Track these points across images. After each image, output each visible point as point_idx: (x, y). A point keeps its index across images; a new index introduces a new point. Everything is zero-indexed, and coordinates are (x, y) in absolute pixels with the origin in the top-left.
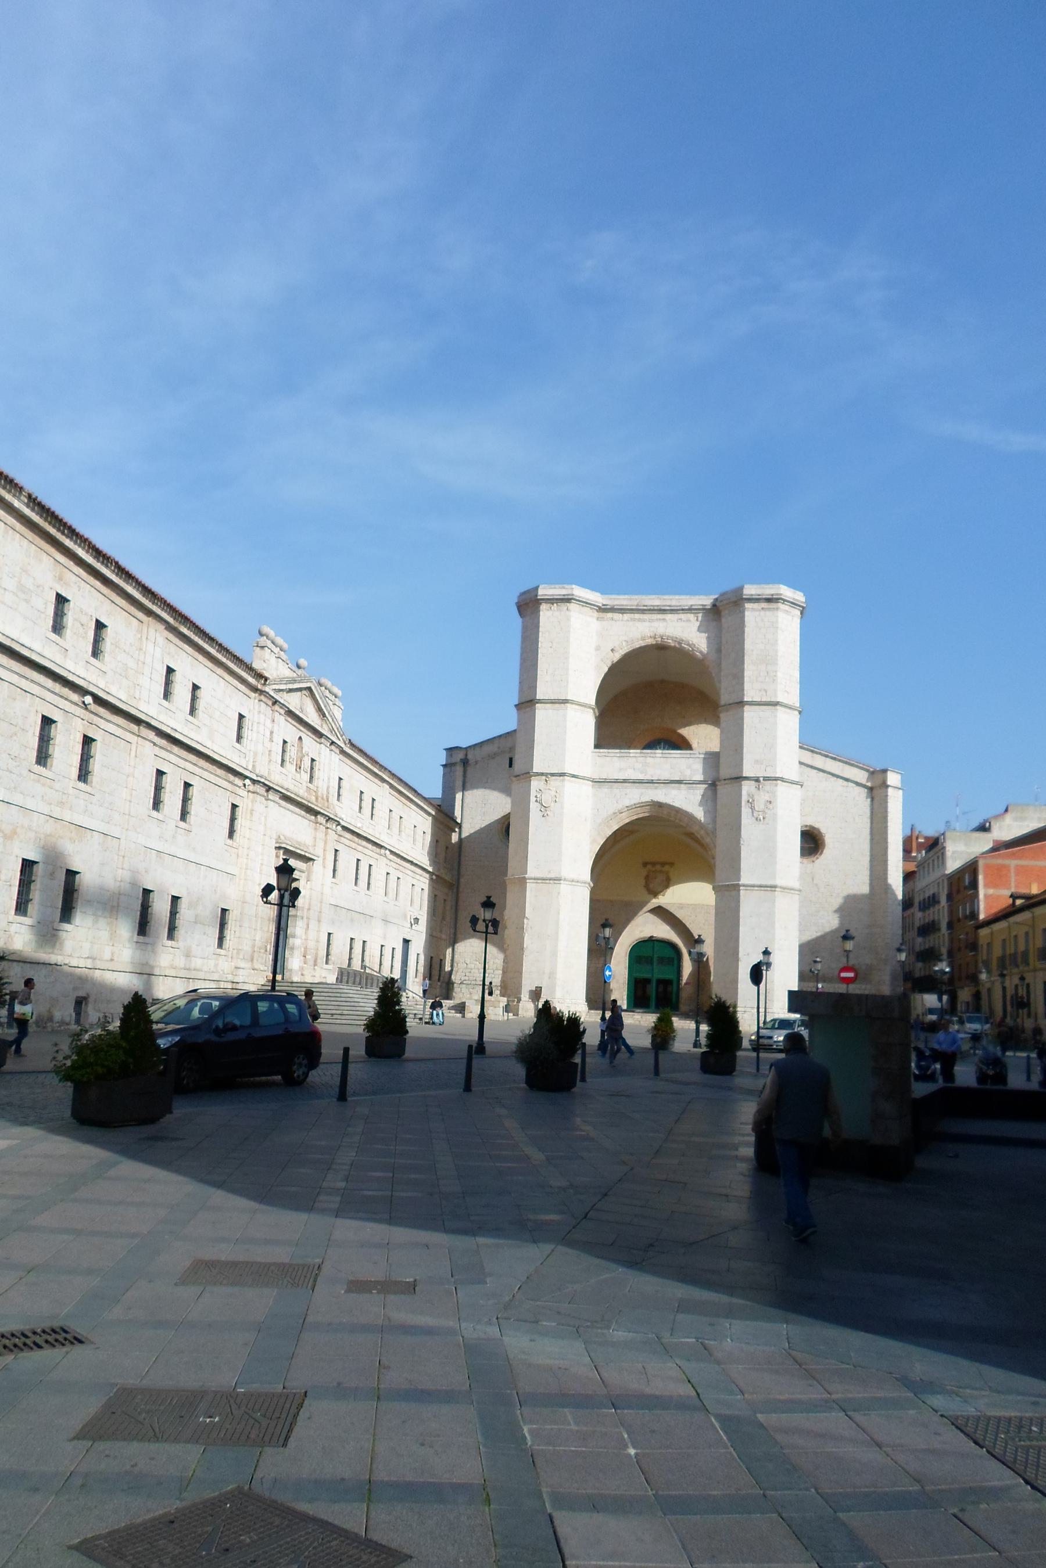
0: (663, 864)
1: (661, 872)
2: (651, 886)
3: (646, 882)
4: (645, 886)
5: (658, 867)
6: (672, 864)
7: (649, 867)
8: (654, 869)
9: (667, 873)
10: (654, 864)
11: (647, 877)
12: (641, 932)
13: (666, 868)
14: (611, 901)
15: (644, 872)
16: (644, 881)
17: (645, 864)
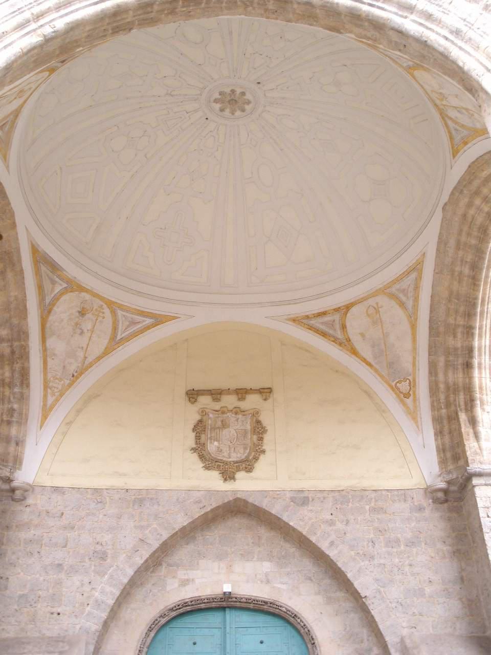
0: (242, 393)
1: (237, 411)
2: (212, 447)
3: (198, 438)
4: (194, 450)
5: (230, 401)
6: (266, 392)
7: (205, 401)
8: (217, 406)
9: (256, 414)
10: (215, 394)
11: (199, 428)
12: (185, 583)
13: (252, 401)
14: (96, 490)
15: (192, 414)
16: (192, 435)
17: (193, 395)
